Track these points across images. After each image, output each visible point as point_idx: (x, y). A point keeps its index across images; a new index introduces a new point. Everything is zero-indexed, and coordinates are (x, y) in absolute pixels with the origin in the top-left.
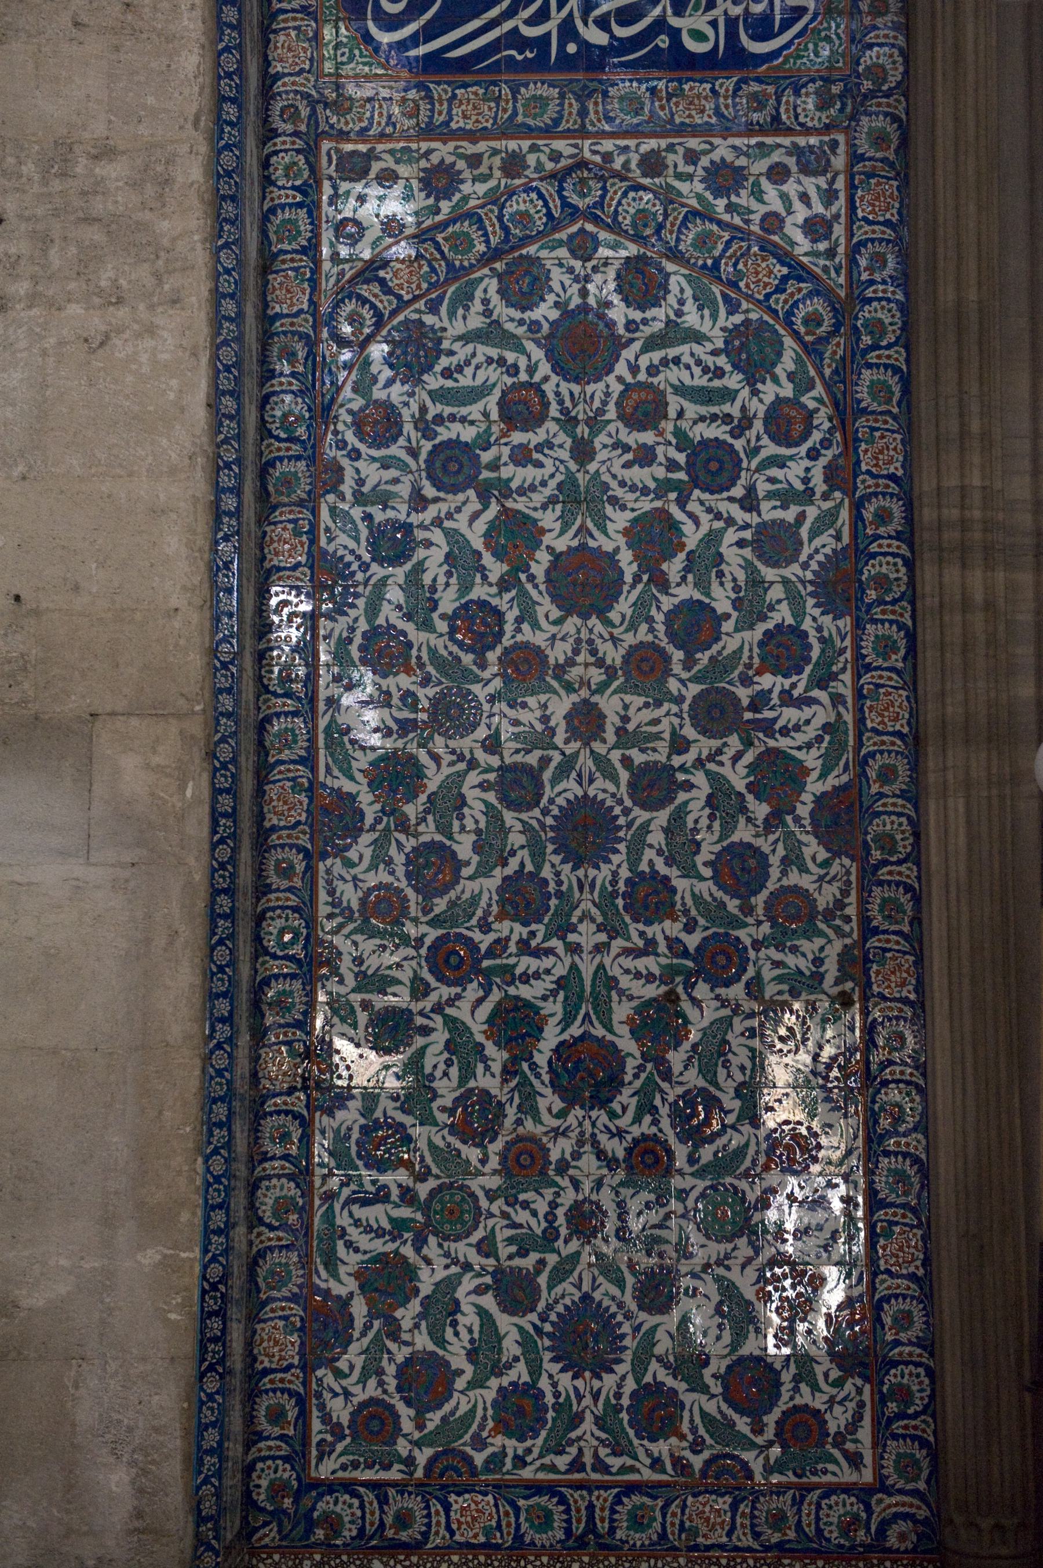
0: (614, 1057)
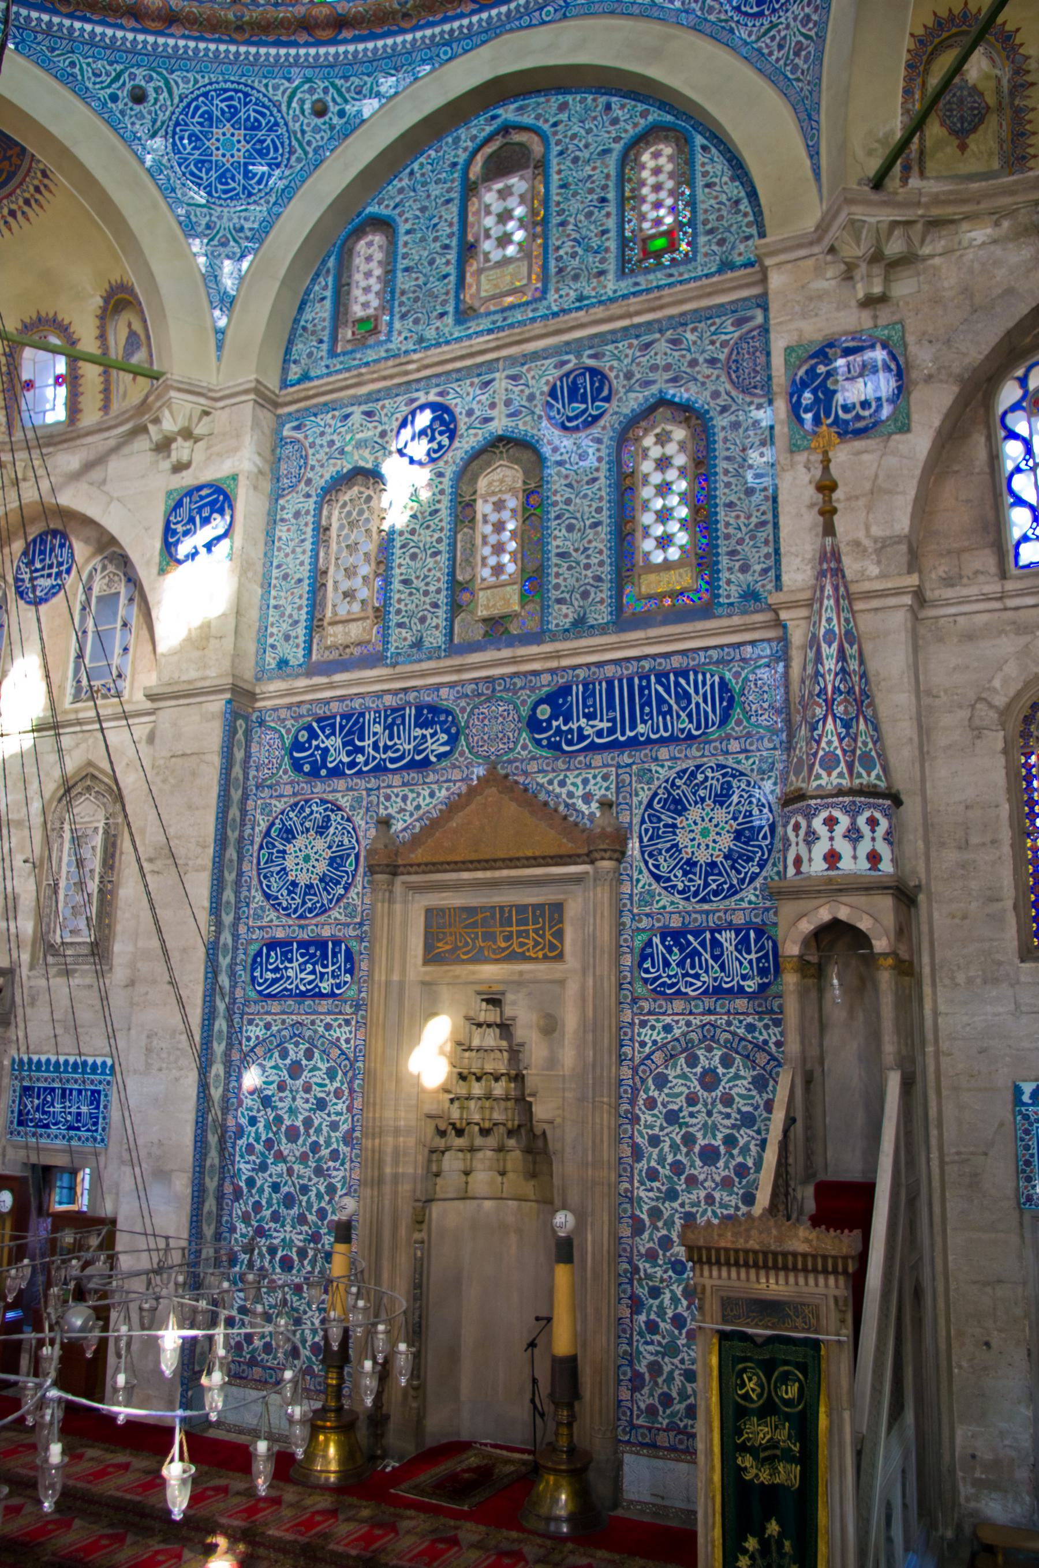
0: (292, 1260)
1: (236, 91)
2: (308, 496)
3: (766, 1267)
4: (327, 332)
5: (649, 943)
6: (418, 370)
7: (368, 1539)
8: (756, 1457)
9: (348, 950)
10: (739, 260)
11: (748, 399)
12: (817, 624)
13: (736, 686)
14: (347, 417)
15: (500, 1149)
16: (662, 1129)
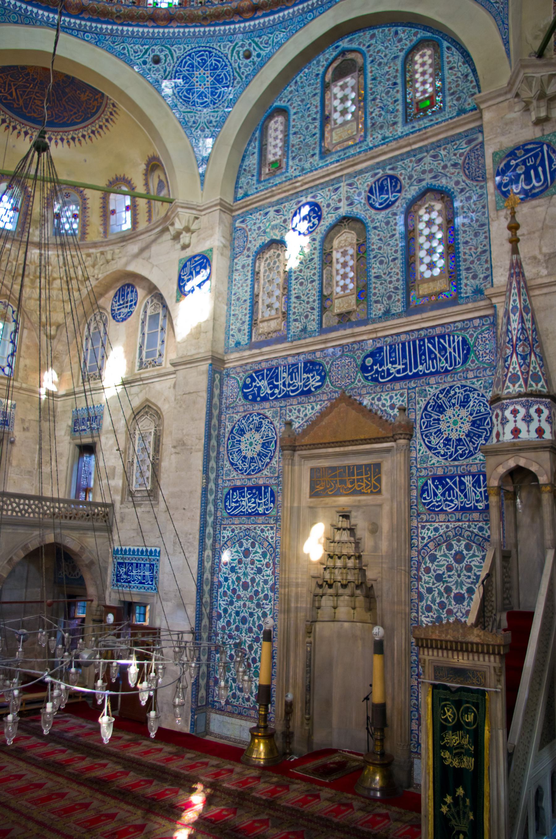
1: (205, 51)
2: (248, 256)
3: (456, 650)
4: (256, 171)
5: (426, 484)
6: (302, 186)
7: (273, 792)
8: (451, 753)
9: (272, 490)
10: (468, 107)
11: (475, 184)
12: (508, 304)
13: (471, 341)
14: (266, 214)
15: (352, 595)
16: (434, 584)
